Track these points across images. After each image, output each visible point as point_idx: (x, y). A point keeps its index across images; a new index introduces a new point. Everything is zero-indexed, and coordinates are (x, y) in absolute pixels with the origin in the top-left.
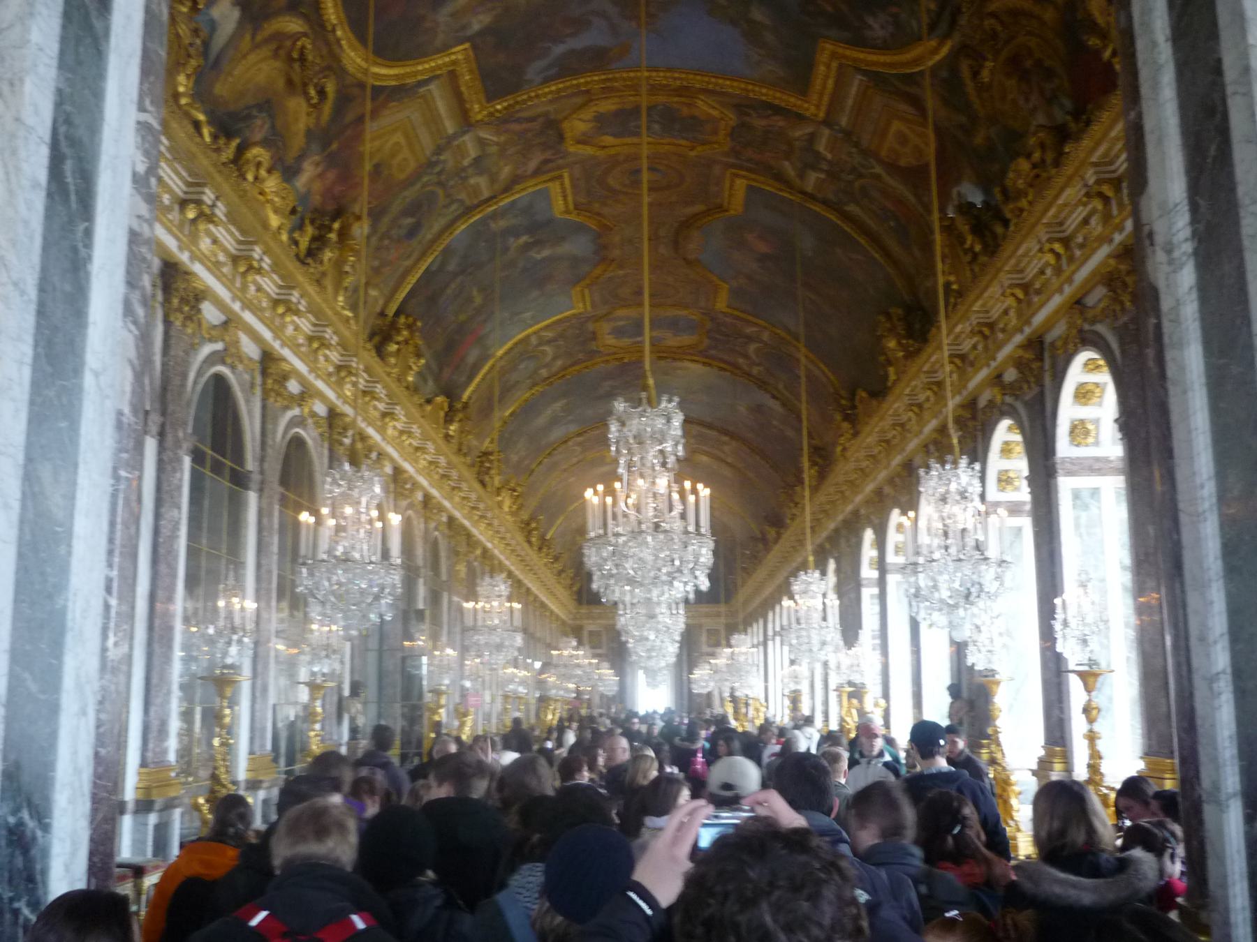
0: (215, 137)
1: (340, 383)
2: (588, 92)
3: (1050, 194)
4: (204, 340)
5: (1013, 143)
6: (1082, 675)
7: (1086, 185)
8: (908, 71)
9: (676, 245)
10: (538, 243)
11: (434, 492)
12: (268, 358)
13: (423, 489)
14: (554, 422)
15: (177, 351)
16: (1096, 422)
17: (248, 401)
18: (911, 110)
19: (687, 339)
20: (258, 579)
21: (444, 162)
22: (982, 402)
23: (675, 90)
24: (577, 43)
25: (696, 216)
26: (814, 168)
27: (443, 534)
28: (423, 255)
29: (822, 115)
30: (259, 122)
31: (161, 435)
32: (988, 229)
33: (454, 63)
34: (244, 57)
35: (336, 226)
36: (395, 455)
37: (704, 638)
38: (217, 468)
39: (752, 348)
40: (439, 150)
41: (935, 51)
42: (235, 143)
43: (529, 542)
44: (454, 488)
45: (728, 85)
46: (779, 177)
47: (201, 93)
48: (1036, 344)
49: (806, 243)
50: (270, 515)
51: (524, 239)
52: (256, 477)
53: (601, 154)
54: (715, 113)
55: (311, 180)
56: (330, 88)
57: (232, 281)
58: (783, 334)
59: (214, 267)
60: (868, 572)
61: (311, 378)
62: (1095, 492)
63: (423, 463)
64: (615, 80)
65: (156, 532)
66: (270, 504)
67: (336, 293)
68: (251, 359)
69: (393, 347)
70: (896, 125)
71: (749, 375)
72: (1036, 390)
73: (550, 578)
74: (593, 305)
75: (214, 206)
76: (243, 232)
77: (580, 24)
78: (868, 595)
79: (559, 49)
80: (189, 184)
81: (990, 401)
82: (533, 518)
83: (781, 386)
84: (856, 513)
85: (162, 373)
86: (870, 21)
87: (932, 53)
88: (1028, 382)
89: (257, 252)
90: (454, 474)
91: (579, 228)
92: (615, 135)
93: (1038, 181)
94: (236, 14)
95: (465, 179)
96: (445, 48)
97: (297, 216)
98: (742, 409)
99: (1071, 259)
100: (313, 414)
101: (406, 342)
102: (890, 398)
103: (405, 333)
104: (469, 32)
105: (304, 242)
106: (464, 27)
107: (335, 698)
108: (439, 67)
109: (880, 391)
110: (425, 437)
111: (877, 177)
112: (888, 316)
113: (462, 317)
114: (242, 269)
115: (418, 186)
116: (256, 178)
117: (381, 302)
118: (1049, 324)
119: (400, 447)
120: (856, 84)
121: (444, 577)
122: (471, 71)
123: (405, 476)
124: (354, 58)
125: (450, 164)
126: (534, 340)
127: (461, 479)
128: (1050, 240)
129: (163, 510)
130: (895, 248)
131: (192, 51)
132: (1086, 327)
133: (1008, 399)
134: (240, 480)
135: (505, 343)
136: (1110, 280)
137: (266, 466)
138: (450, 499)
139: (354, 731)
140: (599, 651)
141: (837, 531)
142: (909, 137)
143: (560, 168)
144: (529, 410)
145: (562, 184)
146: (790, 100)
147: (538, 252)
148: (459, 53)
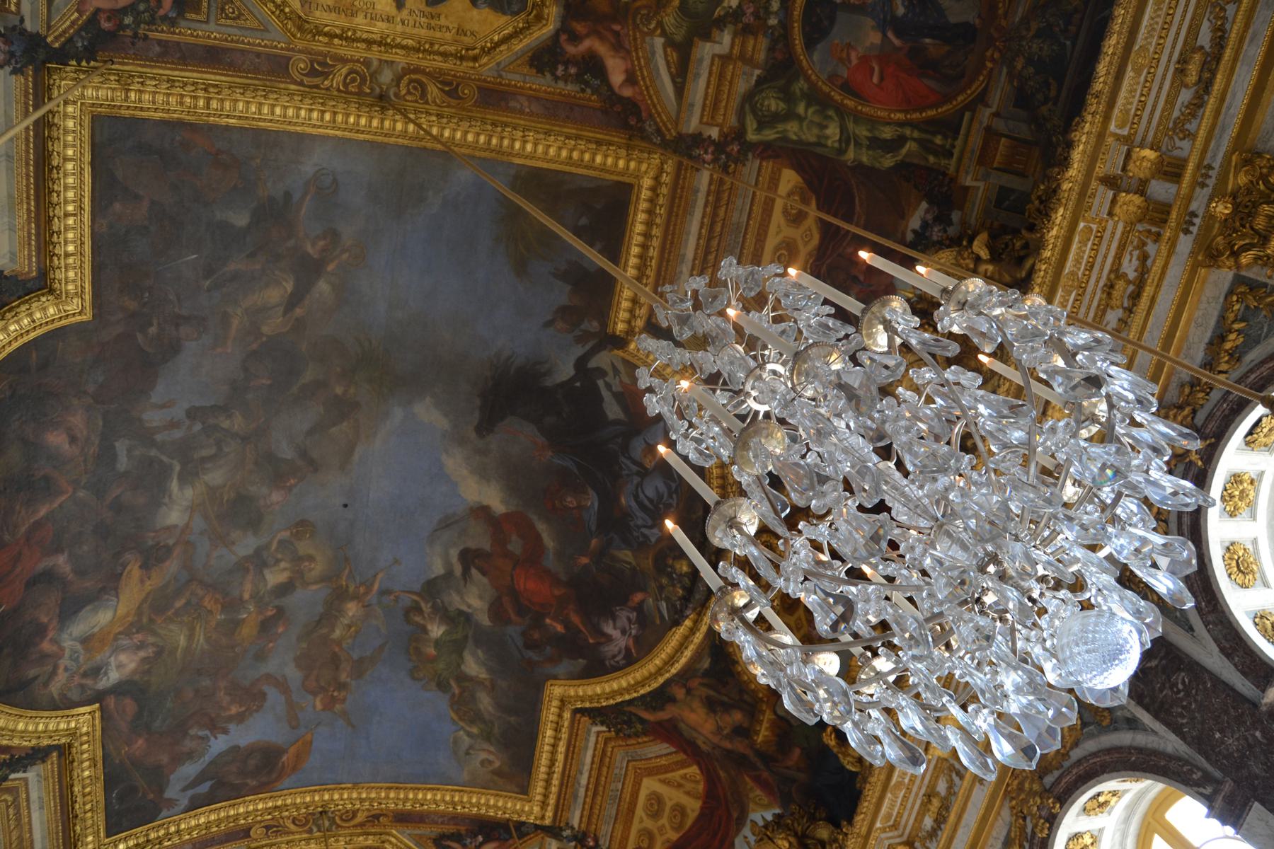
8: (655, 685)
18: (663, 748)
23: (362, 825)
24: (245, 735)
33: (73, 734)
64: (285, 807)
70: (650, 785)
77: (252, 698)
86: (609, 629)
96: (63, 704)
104: (103, 684)
148: (84, 720)
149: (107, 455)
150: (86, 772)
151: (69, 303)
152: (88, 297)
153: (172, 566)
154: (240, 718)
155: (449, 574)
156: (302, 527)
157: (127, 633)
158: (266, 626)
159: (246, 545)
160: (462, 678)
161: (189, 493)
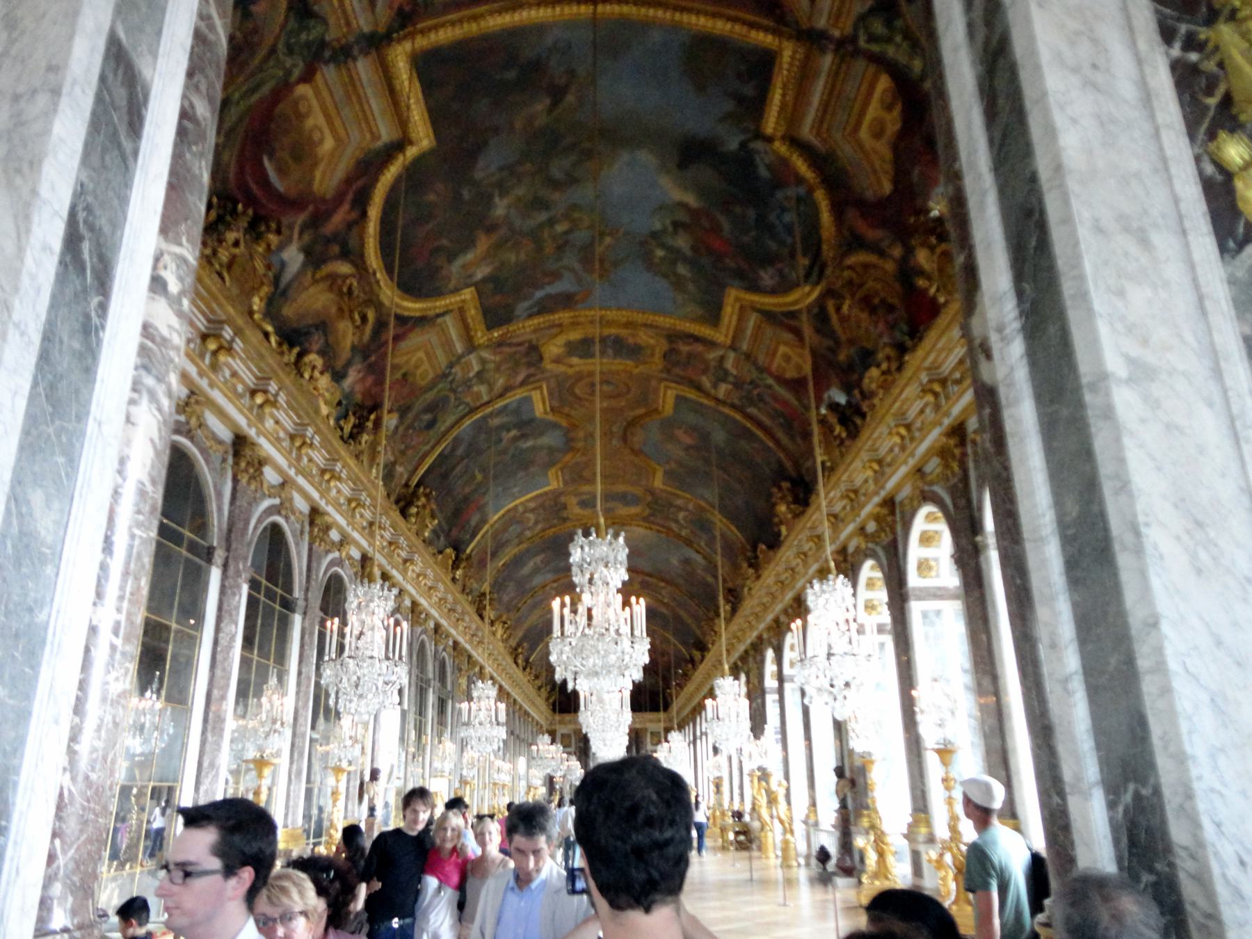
0: (280, 344)
1: (372, 535)
2: (560, 325)
3: (896, 391)
4: (264, 496)
5: (867, 358)
6: (939, 751)
7: (921, 384)
10: (524, 436)
11: (443, 622)
12: (315, 512)
13: (435, 618)
14: (536, 571)
15: (242, 502)
16: (936, 560)
17: (297, 544)
19: (634, 510)
20: (299, 684)
22: (851, 549)
25: (641, 417)
26: (724, 380)
27: (449, 655)
28: (438, 443)
29: (729, 342)
30: (316, 337)
31: (225, 566)
32: (851, 419)
33: (464, 301)
34: (307, 289)
35: (372, 417)
36: (413, 592)
37: (649, 739)
38: (270, 595)
39: (681, 515)
40: (451, 365)
41: (809, 294)
42: (296, 350)
43: (516, 663)
45: (661, 320)
46: (699, 388)
47: (271, 311)
48: (889, 503)
49: (719, 436)
50: (312, 634)
51: (514, 433)
52: (301, 603)
53: (570, 371)
54: (652, 341)
55: (356, 382)
56: (371, 315)
57: (290, 452)
58: (703, 504)
59: (276, 441)
60: (770, 682)
61: (349, 529)
62: (938, 613)
63: (435, 599)
65: (216, 642)
66: (312, 625)
67: (371, 467)
68: (301, 513)
69: (414, 510)
70: (782, 349)
71: (679, 537)
72: (890, 537)
73: (531, 691)
74: (565, 483)
75: (276, 395)
76: (299, 416)
77: (556, 276)
78: (771, 700)
79: (539, 294)
80: (257, 378)
81: (857, 548)
82: (519, 645)
83: (703, 544)
84: (760, 638)
85: (229, 518)
86: (762, 273)
87: (805, 296)
88: (884, 531)
89: (310, 432)
90: (459, 609)
91: (555, 426)
92: (581, 357)
93: (886, 386)
94: (301, 257)
95: (470, 387)
96: (456, 290)
97: (344, 408)
98: (675, 561)
99: (912, 439)
100: (350, 558)
101: (424, 506)
102: (783, 549)
103: (423, 500)
105: (347, 429)
106: (470, 276)
107: (358, 783)
108: (451, 304)
109: (774, 543)
110: (436, 580)
111: (770, 387)
112: (780, 488)
113: (467, 490)
114: (298, 444)
115: (435, 390)
116: (311, 377)
117: (406, 476)
118: (899, 486)
119: (417, 585)
120: (752, 320)
121: (449, 687)
122: (476, 308)
124: (388, 293)
125: (459, 375)
126: (521, 509)
127: (463, 613)
128: (897, 426)
129: (222, 625)
130: (785, 440)
131: (265, 280)
132: (926, 488)
133: (870, 545)
134: (288, 605)
136: (943, 453)
137: (310, 594)
138: (456, 628)
140: (568, 750)
141: (746, 652)
142: (792, 358)
143: (539, 381)
144: (518, 561)
145: (542, 393)
146: (705, 331)
148: (468, 294)
149: (458, 197)
150: (473, 313)
151: (423, 138)
152: (431, 135)
153: (503, 231)
154: (549, 283)
155: (664, 231)
156: (574, 207)
157: (484, 259)
158: (560, 248)
159: (543, 216)
160: (676, 274)
161: (506, 201)
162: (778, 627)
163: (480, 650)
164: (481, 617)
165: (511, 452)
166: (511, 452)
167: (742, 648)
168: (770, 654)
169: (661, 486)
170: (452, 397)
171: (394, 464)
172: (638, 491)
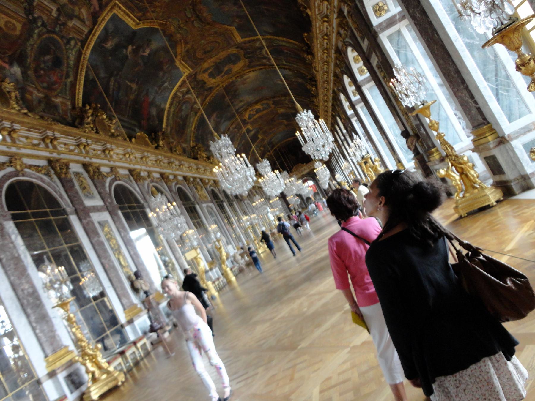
9: (200, 19)
19: (241, 64)
21: (40, 17)
44: (179, 166)
51: (130, 48)
60: (350, 112)
74: (192, 67)
78: (354, 120)
83: (284, 63)
84: (334, 92)
91: (152, 31)
95: (64, 24)
100: (30, 167)
102: (314, 24)
113: (132, 97)
115: (35, 36)
117: (69, 103)
123: (138, 171)
135: (167, 101)
138: (182, 170)
139: (146, 293)
141: (333, 105)
145: (120, 8)
147: (144, 52)
162: (338, 78)
163: (208, 174)
164: (196, 158)
165: (140, 61)
166: (140, 61)
167: (330, 104)
168: (342, 97)
169: (242, 40)
170: (55, 36)
171: (47, 97)
172: (233, 51)
